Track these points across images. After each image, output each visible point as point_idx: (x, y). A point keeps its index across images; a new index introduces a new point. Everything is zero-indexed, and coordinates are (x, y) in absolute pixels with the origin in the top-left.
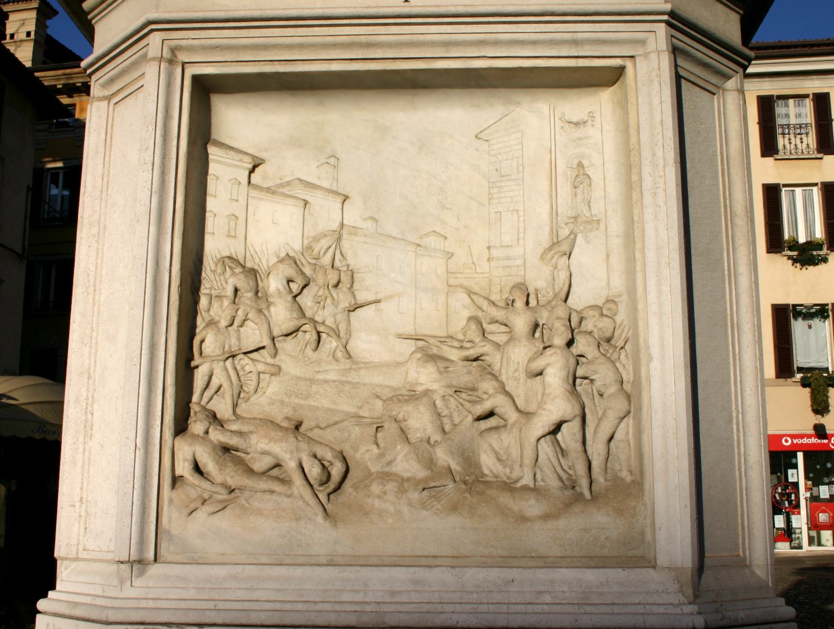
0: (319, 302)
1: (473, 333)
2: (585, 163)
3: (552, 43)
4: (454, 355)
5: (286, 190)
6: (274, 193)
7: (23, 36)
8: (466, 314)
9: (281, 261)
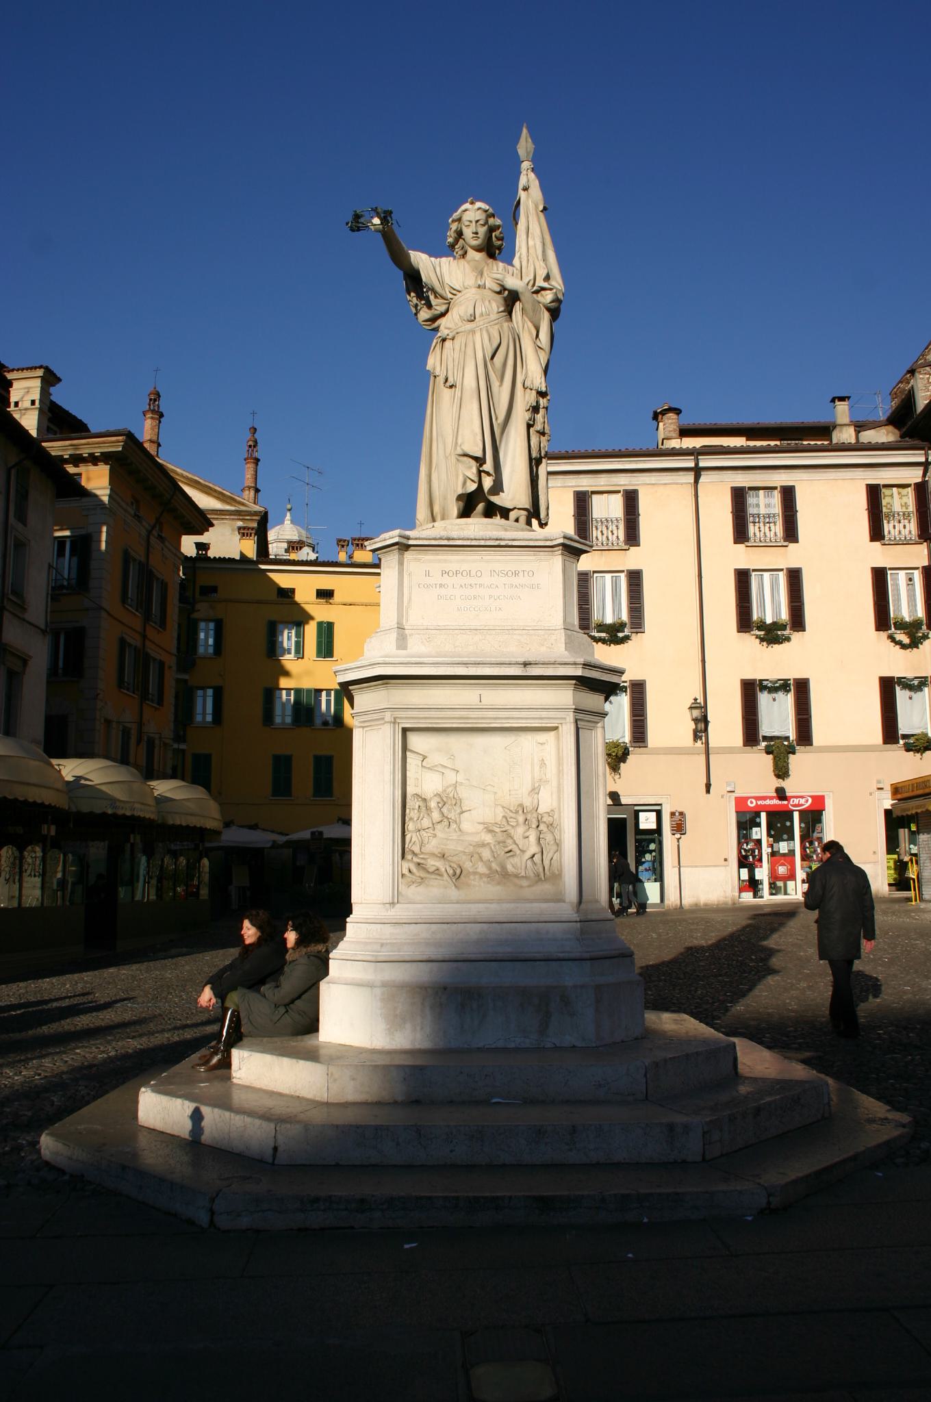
0: (449, 811)
1: (504, 822)
2: (544, 759)
3: (533, 718)
4: (498, 830)
5: (435, 768)
6: (431, 769)
7: (27, 404)
8: (502, 815)
9: (435, 796)
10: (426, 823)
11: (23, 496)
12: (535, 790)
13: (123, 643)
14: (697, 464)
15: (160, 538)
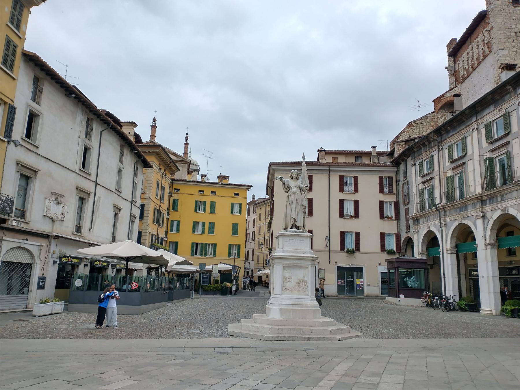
10: (286, 282)
11: (137, 169)
12: (304, 277)
13: (155, 209)
14: (330, 169)
15: (165, 175)
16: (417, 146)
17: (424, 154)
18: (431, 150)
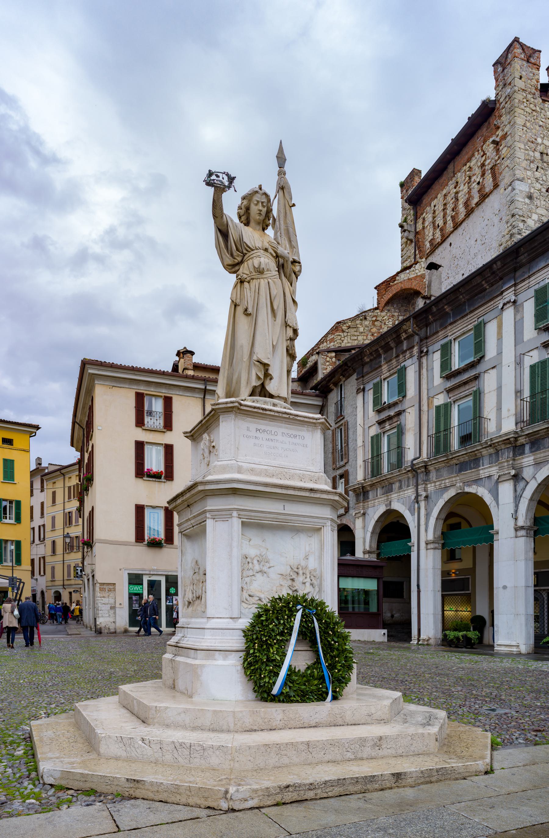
16: (371, 351)
17: (386, 366)
18: (401, 356)
